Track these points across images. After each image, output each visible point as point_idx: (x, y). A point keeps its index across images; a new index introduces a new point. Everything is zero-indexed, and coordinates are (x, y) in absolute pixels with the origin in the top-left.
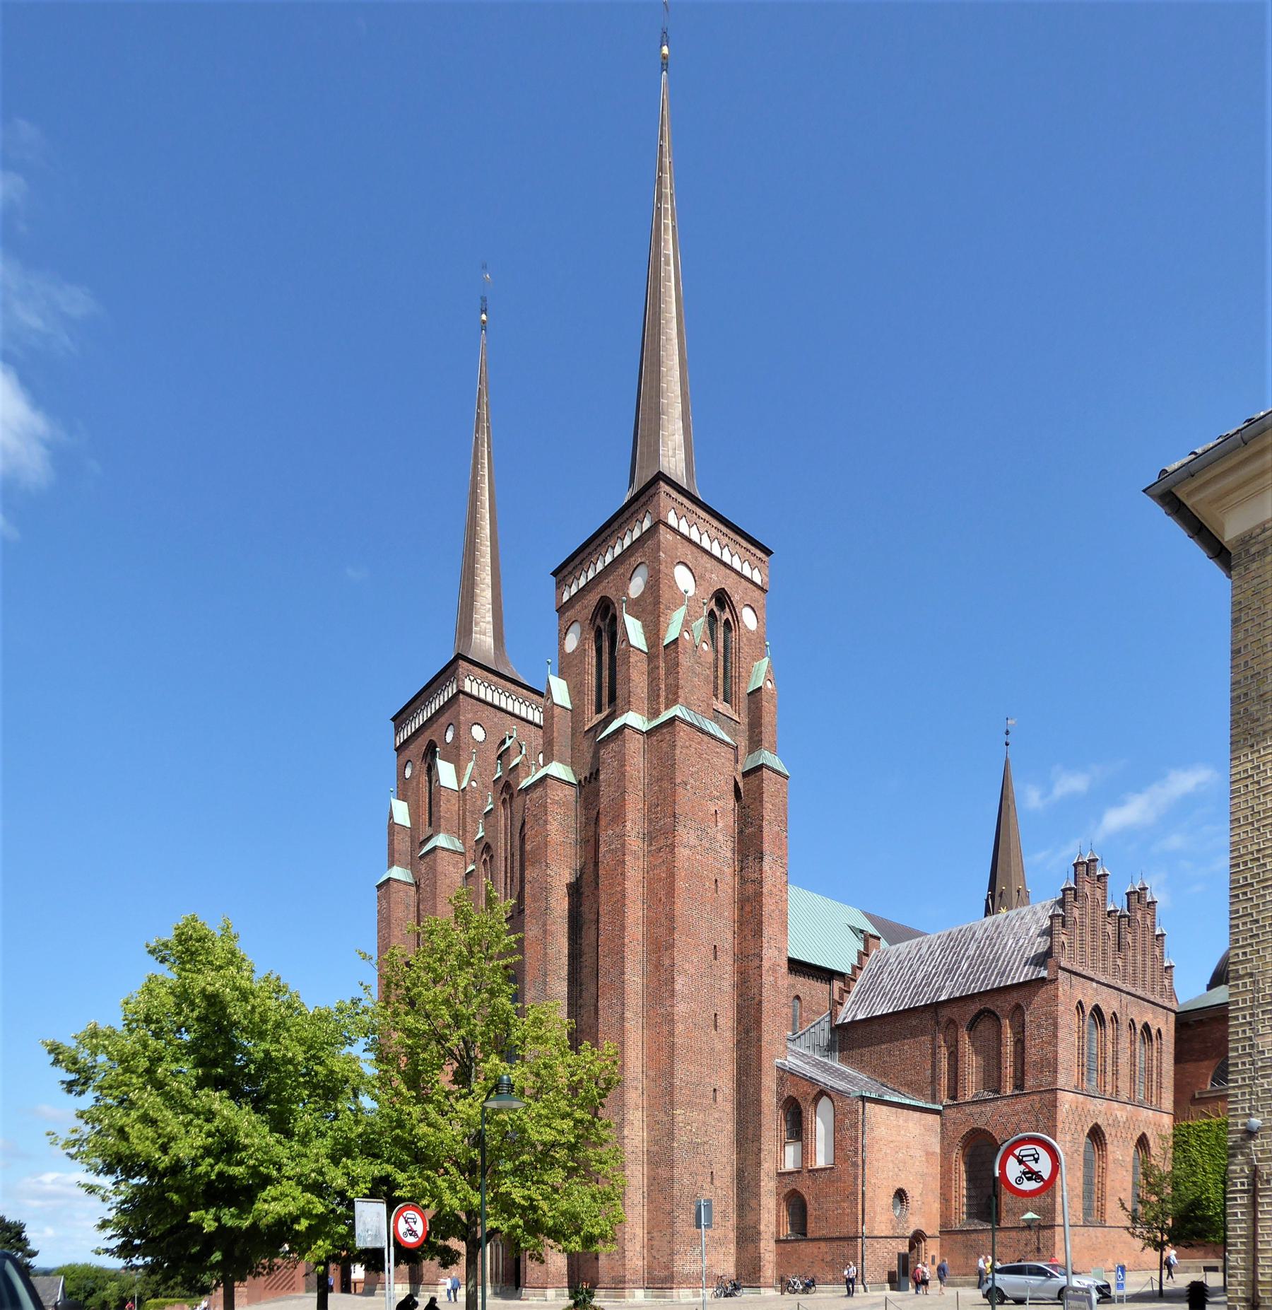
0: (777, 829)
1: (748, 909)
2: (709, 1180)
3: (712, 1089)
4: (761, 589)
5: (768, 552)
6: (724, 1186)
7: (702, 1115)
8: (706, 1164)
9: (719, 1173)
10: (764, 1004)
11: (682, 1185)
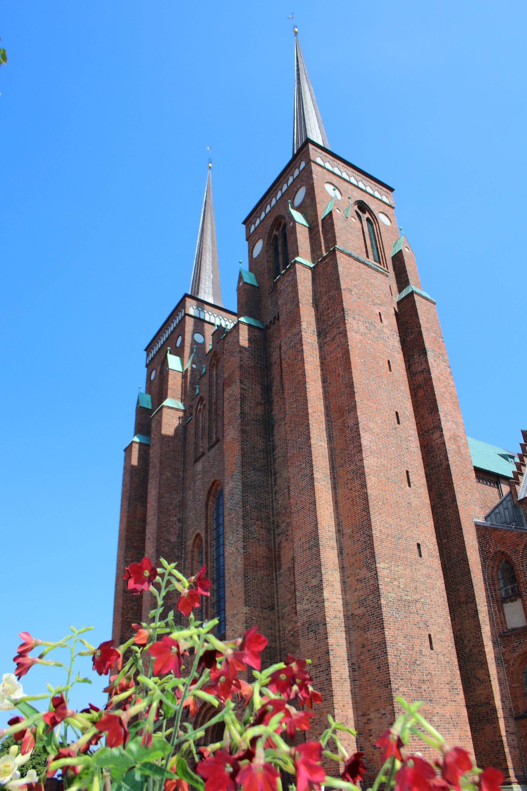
0: (433, 334)
1: (421, 393)
2: (428, 644)
3: (415, 544)
4: (390, 206)
5: (392, 190)
6: (446, 651)
7: (408, 571)
8: (421, 625)
9: (438, 636)
10: (452, 468)
11: (397, 649)
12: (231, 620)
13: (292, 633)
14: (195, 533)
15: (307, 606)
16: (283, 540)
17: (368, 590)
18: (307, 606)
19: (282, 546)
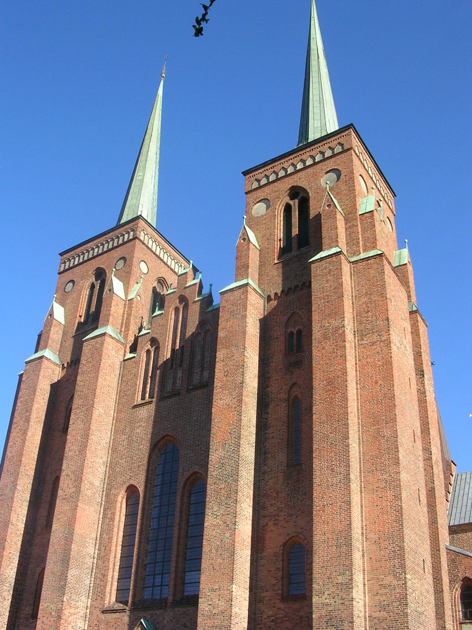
12: (209, 594)
13: (272, 618)
14: (128, 484)
15: (327, 601)
16: (271, 523)
17: (394, 597)
18: (327, 601)
19: (269, 529)
